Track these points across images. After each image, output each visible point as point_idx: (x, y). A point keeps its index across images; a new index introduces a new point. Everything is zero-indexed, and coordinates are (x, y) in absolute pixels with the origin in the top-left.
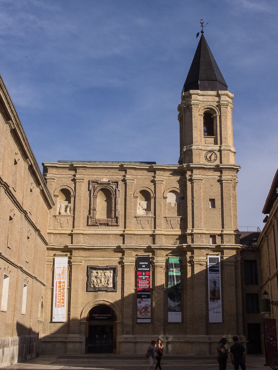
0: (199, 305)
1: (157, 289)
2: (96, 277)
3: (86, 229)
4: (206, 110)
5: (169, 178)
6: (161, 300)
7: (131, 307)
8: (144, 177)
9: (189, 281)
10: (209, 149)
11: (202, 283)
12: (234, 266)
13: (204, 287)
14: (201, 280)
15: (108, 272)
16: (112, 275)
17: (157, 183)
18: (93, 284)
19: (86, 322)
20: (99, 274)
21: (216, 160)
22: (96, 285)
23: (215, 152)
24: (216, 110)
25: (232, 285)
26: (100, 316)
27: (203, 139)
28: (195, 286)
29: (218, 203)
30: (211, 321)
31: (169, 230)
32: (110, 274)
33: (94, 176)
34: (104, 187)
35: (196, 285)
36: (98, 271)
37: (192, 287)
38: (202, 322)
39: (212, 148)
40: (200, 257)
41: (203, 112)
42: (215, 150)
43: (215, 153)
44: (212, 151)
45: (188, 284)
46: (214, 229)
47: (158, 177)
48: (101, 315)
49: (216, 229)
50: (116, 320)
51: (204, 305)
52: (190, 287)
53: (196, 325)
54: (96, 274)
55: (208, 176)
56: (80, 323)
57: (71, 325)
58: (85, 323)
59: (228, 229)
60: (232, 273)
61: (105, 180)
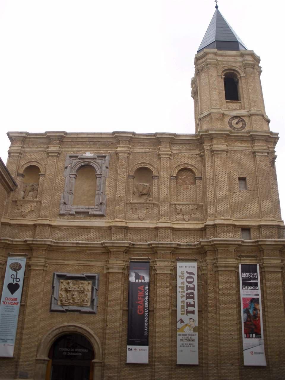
0: (228, 336)
1: (159, 311)
2: (67, 291)
3: (57, 220)
4: (227, 72)
5: (179, 151)
6: (166, 327)
7: (117, 337)
8: (143, 150)
9: (211, 298)
10: (235, 113)
11: (231, 301)
12: (280, 275)
13: (235, 306)
14: (229, 295)
15: (86, 282)
16: (90, 287)
17: (163, 157)
18: (61, 301)
19: (46, 358)
20: (71, 284)
21: (245, 124)
22: (64, 302)
23: (242, 118)
24: (240, 71)
25: (279, 303)
26: (70, 352)
27: (225, 105)
28: (220, 304)
29: (249, 182)
30: (247, 363)
31: (180, 222)
32: (87, 286)
33: (74, 149)
34: (86, 163)
35: (221, 302)
36: (69, 281)
37: (216, 307)
38: (232, 364)
39: (239, 112)
40: (228, 260)
41: (223, 74)
42: (243, 116)
43: (241, 118)
44: (238, 117)
45: (209, 302)
46: (247, 219)
47: (164, 149)
48: (73, 350)
49: (250, 220)
50: (93, 359)
51: (236, 336)
52: (211, 307)
53: (223, 369)
54: (67, 286)
55: (235, 148)
56: (37, 360)
57: (21, 362)
58: (44, 360)
59: (268, 219)
60: (277, 285)
61: (88, 154)
